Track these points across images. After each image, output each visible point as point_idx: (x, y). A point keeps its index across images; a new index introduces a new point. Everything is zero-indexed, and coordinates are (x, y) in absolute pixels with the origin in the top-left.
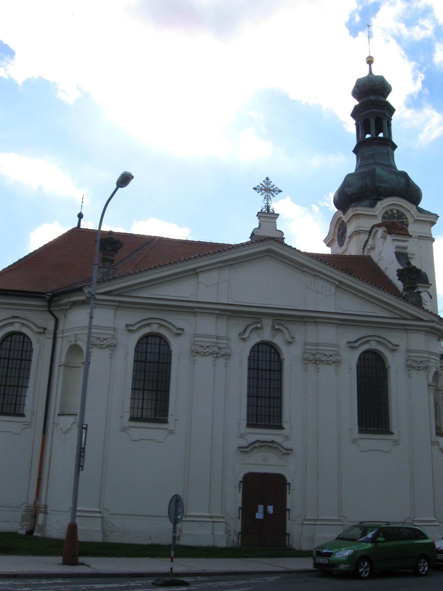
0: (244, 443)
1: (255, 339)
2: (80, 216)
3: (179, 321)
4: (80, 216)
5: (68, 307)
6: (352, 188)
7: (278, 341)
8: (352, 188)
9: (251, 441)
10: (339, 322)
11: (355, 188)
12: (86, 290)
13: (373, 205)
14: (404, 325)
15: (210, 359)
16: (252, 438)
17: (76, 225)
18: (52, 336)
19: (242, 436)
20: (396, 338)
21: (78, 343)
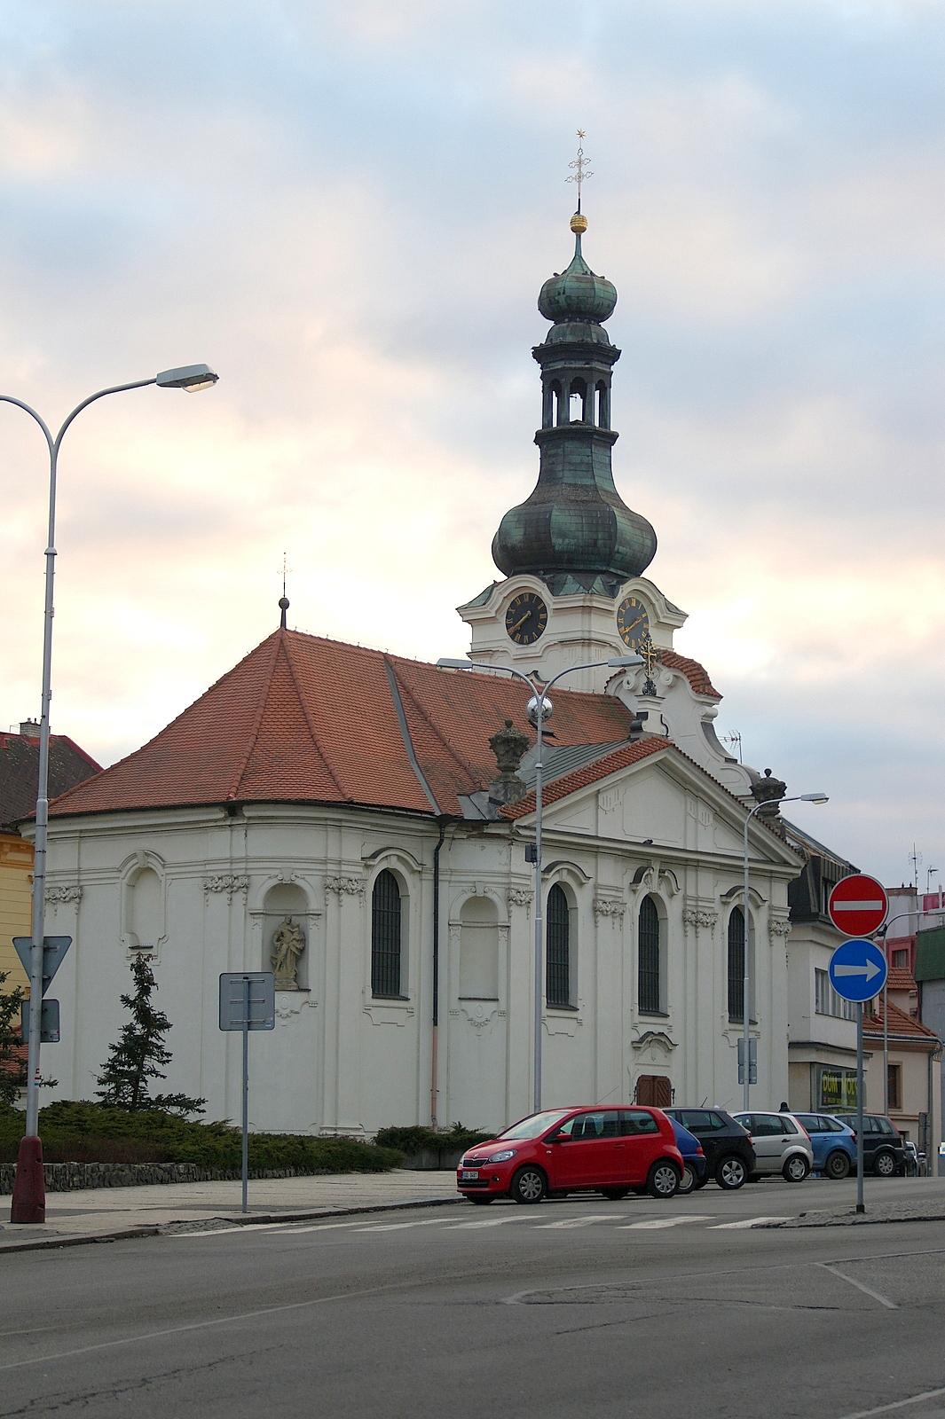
0: (636, 1037)
1: (643, 889)
2: (284, 604)
3: (586, 864)
4: (284, 604)
5: (465, 837)
6: (567, 541)
7: (663, 893)
8: (567, 541)
9: (642, 1034)
10: (718, 867)
11: (573, 542)
12: (515, 824)
13: (612, 592)
14: (771, 872)
15: (610, 918)
16: (643, 1030)
17: (275, 625)
18: (432, 877)
19: (634, 1028)
20: (762, 888)
21: (489, 895)
